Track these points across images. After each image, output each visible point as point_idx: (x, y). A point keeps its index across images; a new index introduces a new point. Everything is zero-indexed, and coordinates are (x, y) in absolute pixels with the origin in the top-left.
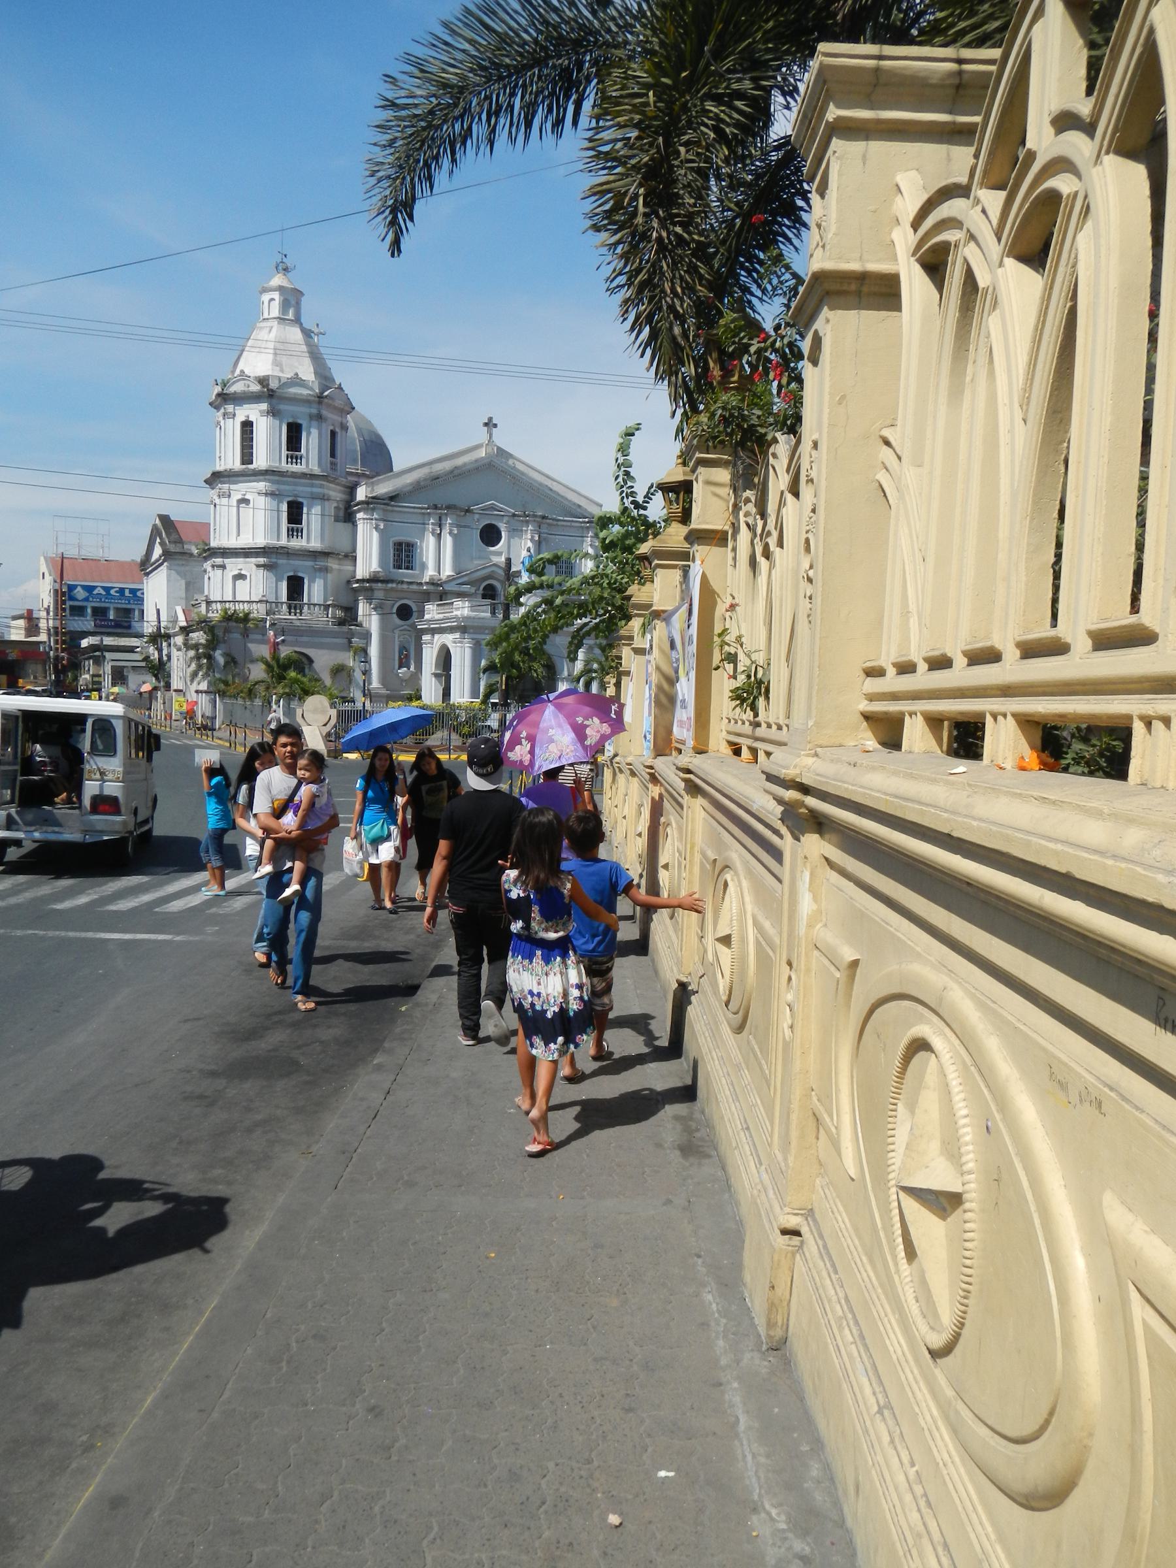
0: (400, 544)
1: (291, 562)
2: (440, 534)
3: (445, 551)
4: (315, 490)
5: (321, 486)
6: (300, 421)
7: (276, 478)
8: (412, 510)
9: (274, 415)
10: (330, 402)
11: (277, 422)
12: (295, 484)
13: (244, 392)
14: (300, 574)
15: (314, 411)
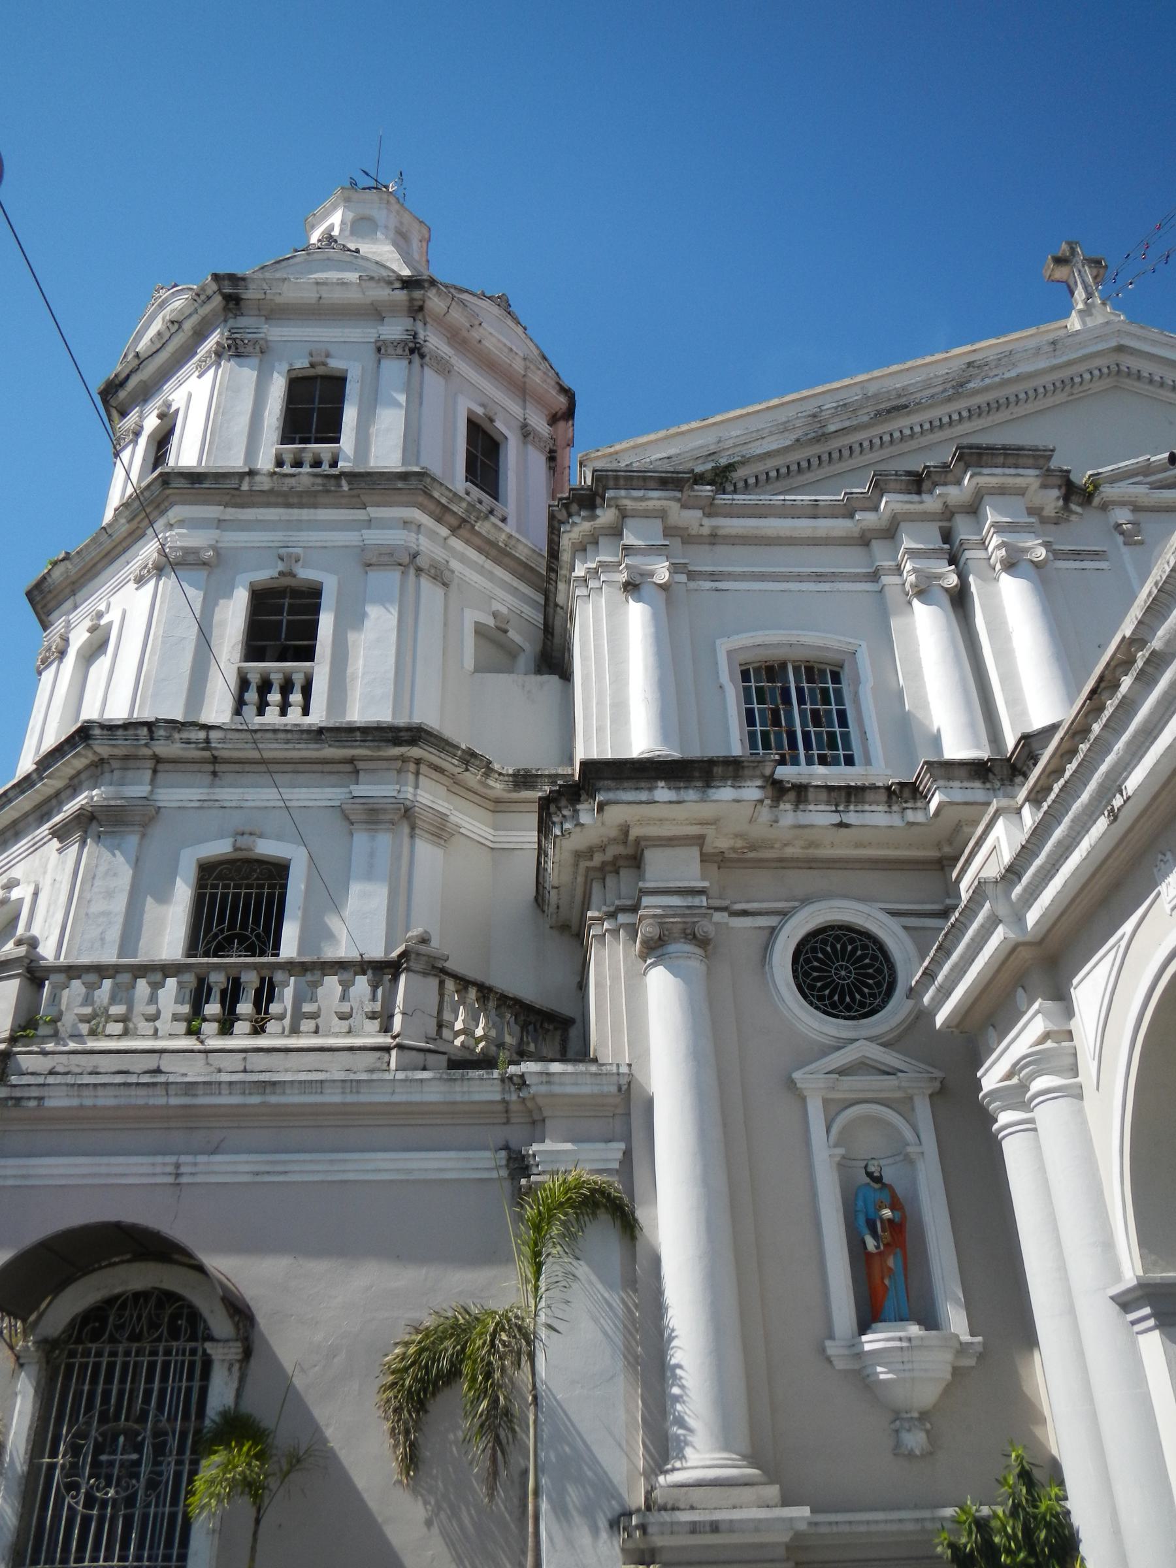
0: (773, 671)
1: (228, 794)
2: (960, 600)
3: (1005, 654)
4: (374, 537)
5: (406, 524)
6: (336, 364)
7: (213, 511)
8: (803, 526)
9: (238, 355)
10: (457, 316)
11: (247, 375)
12: (290, 525)
13: (162, 341)
14: (267, 848)
15: (395, 330)
